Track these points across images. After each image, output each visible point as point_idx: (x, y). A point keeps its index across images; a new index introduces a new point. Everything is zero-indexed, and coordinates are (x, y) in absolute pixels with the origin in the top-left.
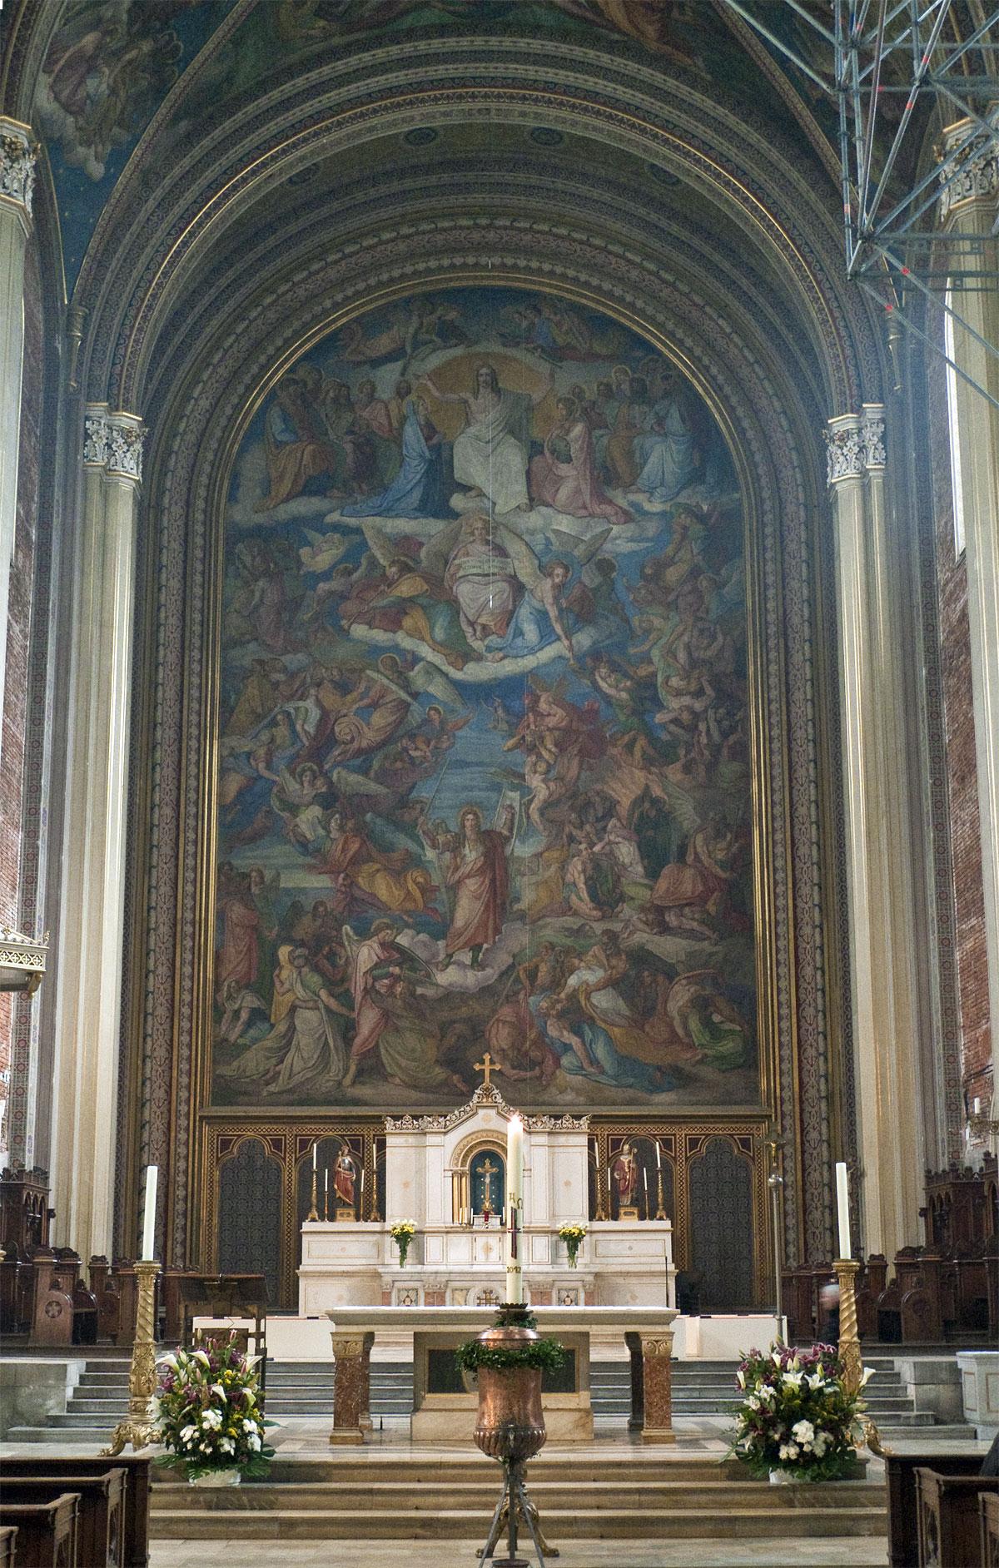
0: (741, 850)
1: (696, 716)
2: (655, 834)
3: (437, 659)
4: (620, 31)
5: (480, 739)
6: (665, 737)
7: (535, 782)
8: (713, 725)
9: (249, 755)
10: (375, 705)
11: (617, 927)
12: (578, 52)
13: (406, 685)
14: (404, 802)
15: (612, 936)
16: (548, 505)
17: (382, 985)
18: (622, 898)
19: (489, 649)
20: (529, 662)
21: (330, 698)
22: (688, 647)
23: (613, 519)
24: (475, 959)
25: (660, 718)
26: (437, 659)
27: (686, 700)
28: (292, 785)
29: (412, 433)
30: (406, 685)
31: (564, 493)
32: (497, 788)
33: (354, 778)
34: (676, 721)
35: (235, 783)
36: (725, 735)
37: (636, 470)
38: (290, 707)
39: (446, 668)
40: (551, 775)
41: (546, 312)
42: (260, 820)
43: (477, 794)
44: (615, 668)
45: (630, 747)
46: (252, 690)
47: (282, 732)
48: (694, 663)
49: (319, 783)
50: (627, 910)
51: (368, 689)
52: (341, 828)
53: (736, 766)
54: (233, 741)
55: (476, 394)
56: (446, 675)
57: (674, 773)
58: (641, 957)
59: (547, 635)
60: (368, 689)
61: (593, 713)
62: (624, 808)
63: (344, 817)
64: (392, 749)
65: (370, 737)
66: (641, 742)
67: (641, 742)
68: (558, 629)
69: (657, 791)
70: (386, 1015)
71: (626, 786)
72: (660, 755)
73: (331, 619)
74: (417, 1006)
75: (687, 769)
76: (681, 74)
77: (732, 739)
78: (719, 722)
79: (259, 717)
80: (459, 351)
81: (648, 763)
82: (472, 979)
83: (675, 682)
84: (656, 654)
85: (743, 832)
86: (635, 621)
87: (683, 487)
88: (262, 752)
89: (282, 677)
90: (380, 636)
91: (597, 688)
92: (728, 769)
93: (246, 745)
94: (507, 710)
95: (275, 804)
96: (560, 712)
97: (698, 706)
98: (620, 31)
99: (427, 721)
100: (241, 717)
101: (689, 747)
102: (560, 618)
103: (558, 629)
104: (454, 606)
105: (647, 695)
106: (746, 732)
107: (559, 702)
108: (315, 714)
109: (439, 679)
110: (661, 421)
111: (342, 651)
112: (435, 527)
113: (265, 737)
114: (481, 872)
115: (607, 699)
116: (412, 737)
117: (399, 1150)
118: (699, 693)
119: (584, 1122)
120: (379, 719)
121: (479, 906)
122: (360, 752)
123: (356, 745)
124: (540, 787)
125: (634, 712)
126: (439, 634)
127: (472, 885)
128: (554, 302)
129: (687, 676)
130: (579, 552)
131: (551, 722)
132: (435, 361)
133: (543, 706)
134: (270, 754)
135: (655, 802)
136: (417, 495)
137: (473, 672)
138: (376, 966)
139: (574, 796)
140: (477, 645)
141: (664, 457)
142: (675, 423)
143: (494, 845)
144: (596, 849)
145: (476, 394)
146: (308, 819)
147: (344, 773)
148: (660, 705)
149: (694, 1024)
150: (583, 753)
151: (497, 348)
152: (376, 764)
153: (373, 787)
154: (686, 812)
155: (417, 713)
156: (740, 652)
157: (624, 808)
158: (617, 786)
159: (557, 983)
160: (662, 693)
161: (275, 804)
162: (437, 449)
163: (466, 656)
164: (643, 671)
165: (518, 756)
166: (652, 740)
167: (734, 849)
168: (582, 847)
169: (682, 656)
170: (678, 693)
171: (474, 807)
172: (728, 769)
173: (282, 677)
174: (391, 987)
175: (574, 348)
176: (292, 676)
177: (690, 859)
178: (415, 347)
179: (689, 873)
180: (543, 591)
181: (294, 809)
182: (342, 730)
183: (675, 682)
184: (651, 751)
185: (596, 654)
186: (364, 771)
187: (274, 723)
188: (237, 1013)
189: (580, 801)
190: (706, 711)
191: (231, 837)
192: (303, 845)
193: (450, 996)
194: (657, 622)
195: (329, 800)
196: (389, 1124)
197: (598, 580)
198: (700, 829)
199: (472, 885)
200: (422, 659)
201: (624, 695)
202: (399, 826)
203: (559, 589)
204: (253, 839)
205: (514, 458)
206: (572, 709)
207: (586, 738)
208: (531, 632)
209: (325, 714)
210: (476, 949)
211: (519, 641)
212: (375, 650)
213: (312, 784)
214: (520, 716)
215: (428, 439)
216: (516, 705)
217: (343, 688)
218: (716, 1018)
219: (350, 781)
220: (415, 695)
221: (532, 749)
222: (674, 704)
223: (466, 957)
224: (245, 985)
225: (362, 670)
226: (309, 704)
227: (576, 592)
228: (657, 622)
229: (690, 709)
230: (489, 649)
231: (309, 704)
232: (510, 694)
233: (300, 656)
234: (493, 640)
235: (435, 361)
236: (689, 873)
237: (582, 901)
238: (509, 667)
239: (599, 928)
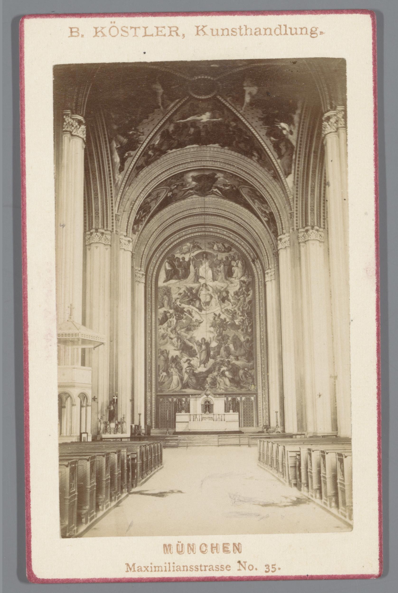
1: (244, 320)
11: (230, 360)
15: (229, 361)
16: (216, 281)
17: (188, 371)
18: (230, 354)
22: (242, 308)
23: (229, 283)
24: (204, 366)
27: (242, 317)
29: (192, 267)
31: (220, 278)
34: (240, 321)
37: (233, 275)
50: (231, 357)
52: (180, 342)
55: (203, 259)
56: (198, 313)
58: (233, 365)
69: (237, 334)
70: (189, 376)
72: (237, 328)
74: (194, 375)
75: (242, 330)
83: (240, 314)
87: (242, 277)
97: (244, 318)
104: (200, 300)
110: (237, 264)
112: (196, 285)
114: (205, 350)
121: (205, 356)
127: (204, 352)
129: (242, 312)
130: (222, 289)
131: (218, 322)
138: (187, 367)
141: (237, 271)
142: (240, 265)
144: (226, 345)
145: (203, 259)
149: (243, 376)
159: (219, 370)
160: (237, 316)
162: (196, 270)
167: (251, 345)
168: (223, 345)
169: (241, 309)
170: (241, 316)
174: (190, 371)
177: (242, 347)
179: (242, 350)
188: (162, 376)
190: (246, 319)
193: (200, 373)
197: (226, 295)
199: (204, 352)
201: (231, 317)
203: (219, 297)
205: (210, 272)
210: (205, 364)
215: (195, 268)
218: (247, 376)
223: (203, 365)
224: (164, 371)
227: (222, 297)
236: (242, 350)
239: (227, 360)
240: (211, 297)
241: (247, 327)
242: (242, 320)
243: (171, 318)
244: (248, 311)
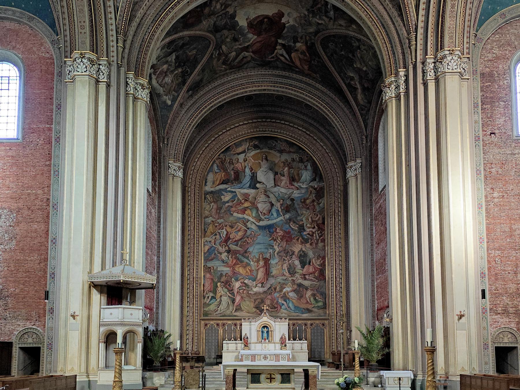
0: (323, 262)
1: (313, 233)
2: (304, 261)
3: (254, 221)
4: (298, 68)
5: (262, 238)
6: (306, 237)
7: (276, 247)
8: (317, 235)
9: (210, 242)
10: (239, 231)
12: (287, 74)
13: (246, 226)
14: (246, 252)
19: (265, 218)
20: (275, 221)
21: (229, 229)
22: (311, 217)
25: (305, 233)
26: (254, 221)
27: (311, 229)
28: (220, 248)
30: (246, 226)
32: (267, 249)
33: (234, 246)
34: (308, 234)
35: (207, 248)
36: (320, 237)
38: (219, 231)
39: (255, 222)
40: (280, 245)
41: (279, 142)
42: (213, 255)
43: (263, 250)
44: (294, 222)
45: (298, 240)
46: (211, 227)
47: (218, 236)
48: (313, 221)
49: (227, 247)
51: (237, 227)
53: (322, 244)
54: (207, 239)
57: (308, 245)
59: (278, 215)
60: (237, 227)
61: (289, 233)
62: (296, 253)
63: (232, 255)
64: (243, 240)
65: (238, 238)
66: (300, 238)
67: (300, 238)
68: (281, 213)
69: (304, 249)
71: (297, 248)
72: (305, 241)
73: (228, 211)
75: (311, 244)
76: (313, 79)
77: (321, 238)
78: (318, 234)
79: (212, 233)
80: (258, 151)
81: (302, 243)
82: (261, 290)
83: (308, 225)
84: (304, 219)
85: (324, 258)
86: (299, 212)
88: (213, 241)
89: (217, 225)
90: (240, 216)
91: (290, 227)
92: (320, 245)
93: (208, 239)
94: (269, 232)
95: (216, 252)
96: (282, 232)
97: (314, 230)
98: (298, 68)
99: (251, 234)
100: (208, 233)
101: (311, 240)
102: (282, 211)
103: (281, 213)
105: (302, 228)
106: (324, 236)
107: (281, 230)
108: (225, 233)
109: (254, 225)
111: (231, 219)
113: (214, 238)
115: (292, 229)
116: (248, 238)
117: (246, 326)
118: (314, 228)
119: (287, 320)
120: (240, 234)
122: (236, 241)
123: (234, 240)
124: (277, 250)
125: (299, 232)
126: (254, 215)
128: (280, 139)
129: (311, 224)
131: (279, 234)
132: (253, 153)
133: (278, 231)
134: (215, 241)
135: (303, 251)
136: (249, 183)
137: (261, 223)
139: (285, 250)
140: (263, 217)
143: (267, 261)
146: (224, 256)
147: (232, 246)
148: (305, 230)
150: (287, 241)
151: (268, 150)
152: (239, 244)
153: (238, 248)
154: (311, 254)
155: (249, 232)
156: (324, 219)
157: (296, 253)
158: (295, 248)
160: (305, 228)
161: (216, 252)
163: (260, 220)
164: (301, 223)
165: (272, 241)
166: (303, 238)
169: (310, 219)
170: (309, 228)
171: (262, 253)
172: (320, 245)
173: (217, 225)
175: (285, 150)
176: (220, 224)
178: (248, 150)
180: (278, 205)
181: (221, 254)
182: (231, 236)
183: (308, 225)
184: (302, 240)
185: (290, 219)
186: (237, 245)
187: (216, 235)
189: (286, 252)
191: (207, 260)
192: (223, 261)
194: (304, 212)
195: (229, 251)
196: (243, 320)
198: (314, 258)
200: (249, 221)
201: (297, 228)
202: (245, 257)
204: (212, 260)
206: (285, 232)
207: (288, 237)
208: (275, 214)
209: (227, 232)
211: (272, 216)
212: (240, 218)
213: (225, 248)
214: (273, 233)
216: (271, 230)
217: (232, 227)
219: (233, 247)
220: (248, 229)
221: (275, 240)
222: (308, 230)
225: (236, 223)
226: (224, 230)
228: (304, 212)
229: (312, 231)
230: (265, 218)
231: (224, 230)
232: (270, 228)
233: (222, 220)
234: (266, 216)
235: (253, 153)
237: (287, 274)
238: (270, 222)
240: (272, 205)
241: (318, 240)
242: (311, 233)
243: (219, 229)
244: (318, 222)
